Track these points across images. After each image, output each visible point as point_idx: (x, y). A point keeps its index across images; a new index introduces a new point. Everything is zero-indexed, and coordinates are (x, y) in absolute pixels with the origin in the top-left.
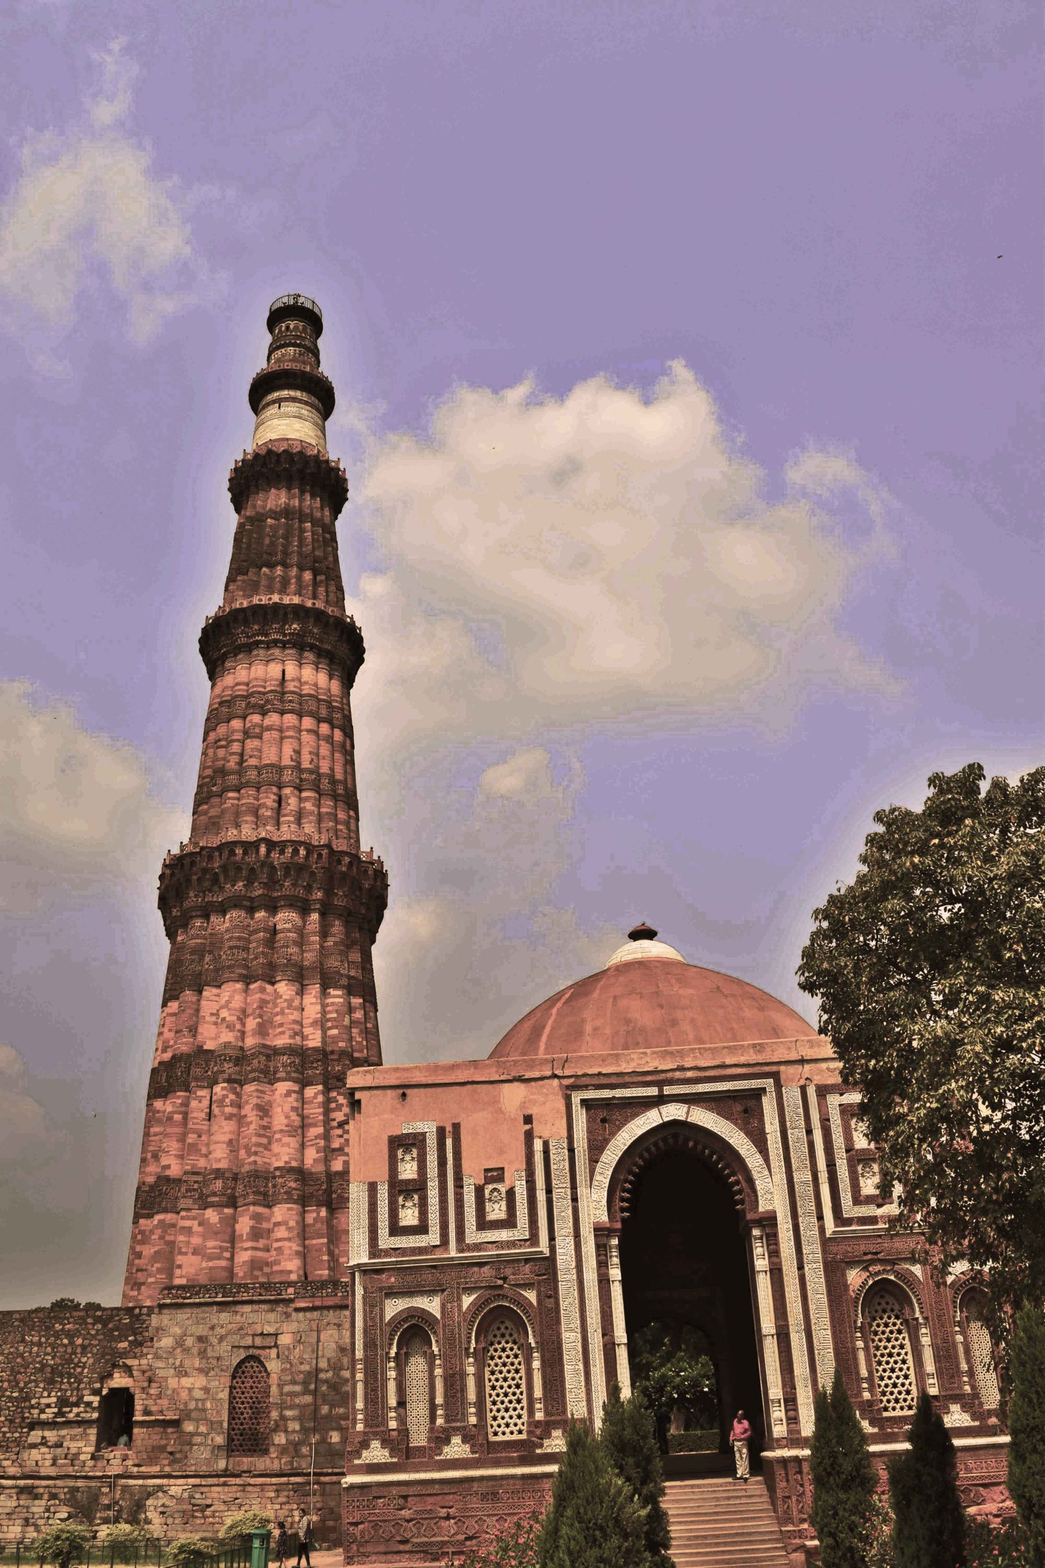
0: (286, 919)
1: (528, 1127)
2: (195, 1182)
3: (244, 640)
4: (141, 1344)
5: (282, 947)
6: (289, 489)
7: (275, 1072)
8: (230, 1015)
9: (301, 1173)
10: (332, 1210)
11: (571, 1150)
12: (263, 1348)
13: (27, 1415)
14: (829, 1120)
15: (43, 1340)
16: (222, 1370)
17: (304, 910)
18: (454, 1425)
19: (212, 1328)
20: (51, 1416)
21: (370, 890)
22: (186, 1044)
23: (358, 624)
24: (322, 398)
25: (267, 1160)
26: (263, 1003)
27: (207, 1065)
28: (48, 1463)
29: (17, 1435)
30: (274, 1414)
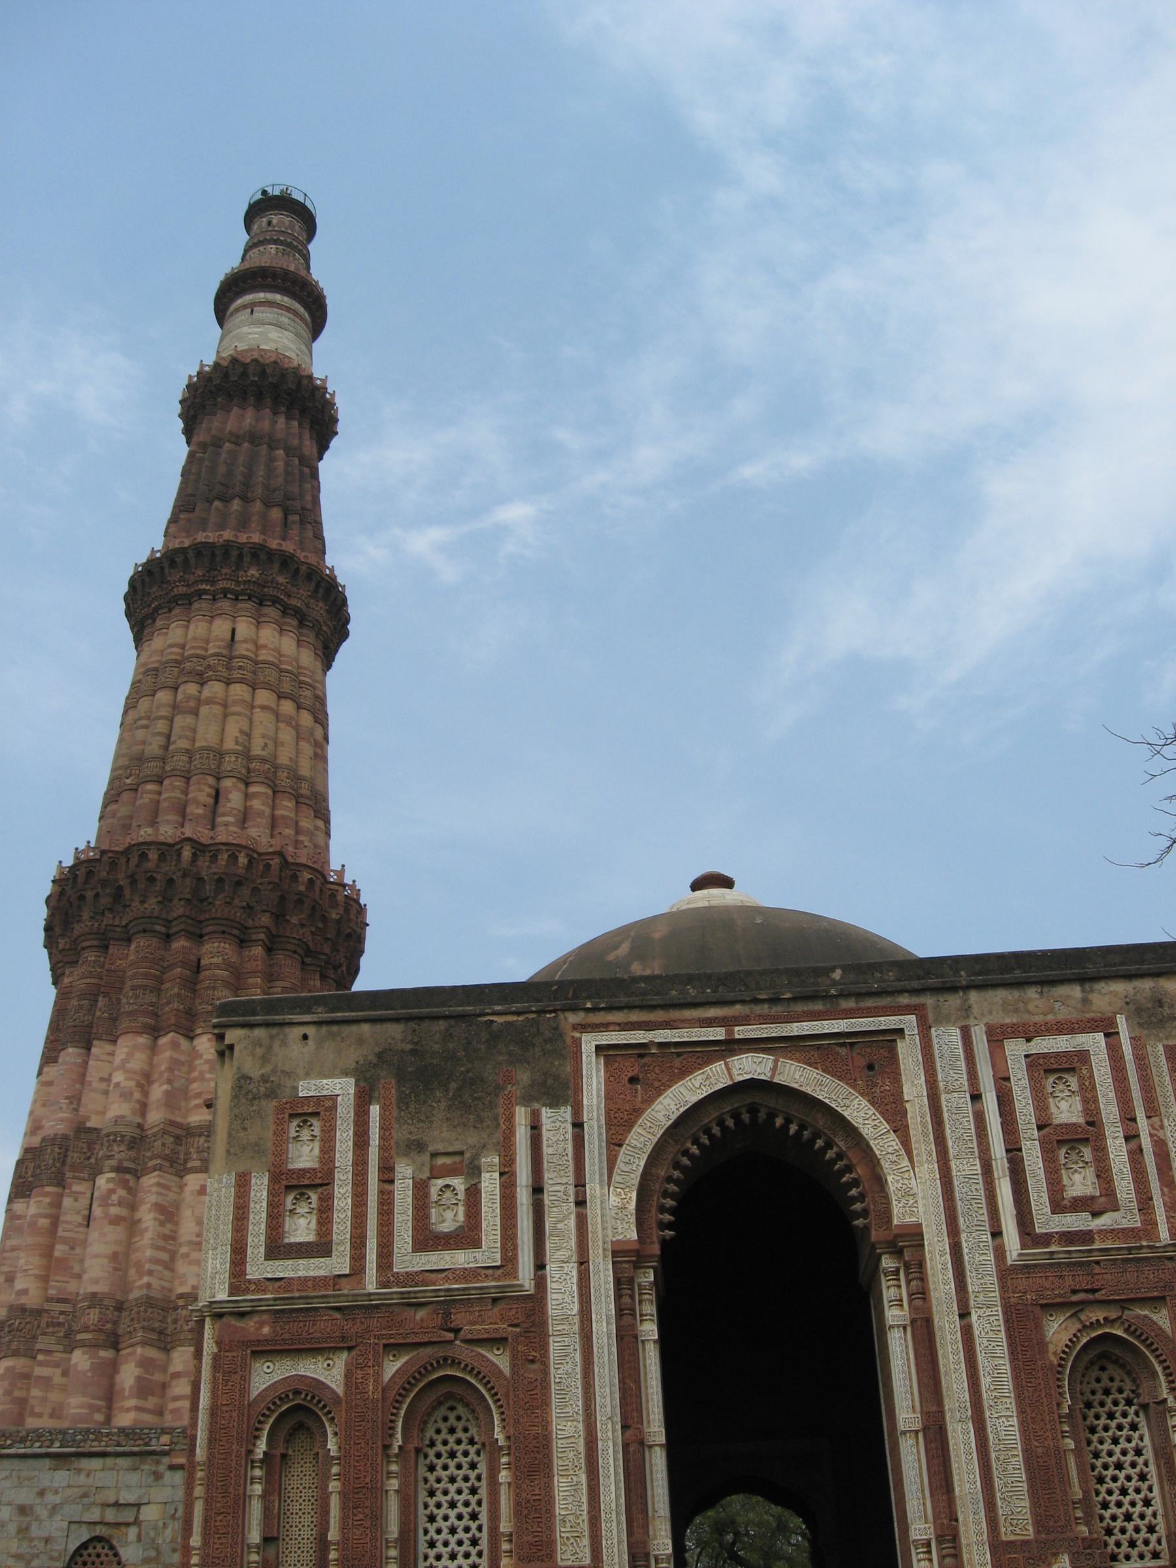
0: (216, 953)
2: (61, 1313)
3: (182, 590)
5: (208, 988)
6: (258, 407)
7: (186, 1161)
8: (126, 1079)
12: (118, 1525)
14: (1008, 1079)
16: (52, 1558)
17: (242, 941)
19: (41, 1493)
21: (339, 921)
22: (62, 1120)
23: (340, 580)
24: (313, 309)
25: (167, 1285)
26: (174, 1064)
27: (89, 1149)
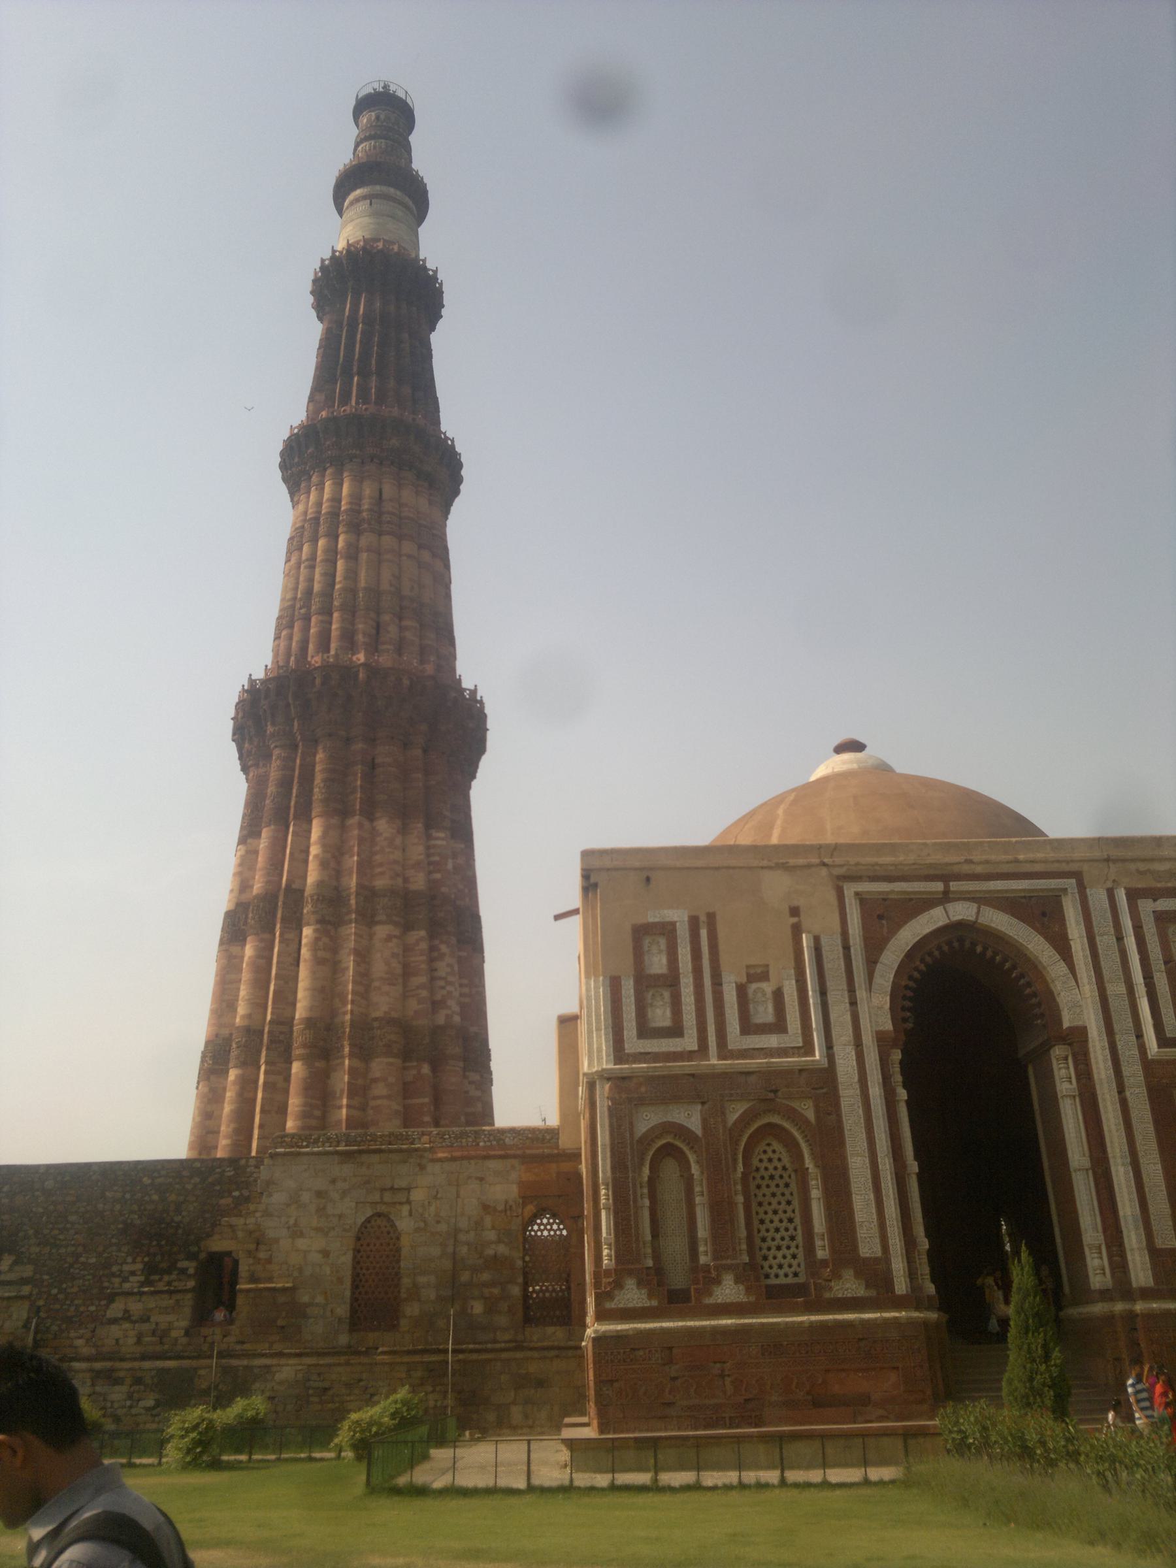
1: (795, 920)
2: (281, 1033)
4: (247, 1200)
9: (404, 1028)
10: (434, 1070)
11: (846, 948)
13: (106, 1284)
15: (128, 1196)
16: (345, 1230)
18: (724, 1262)
19: (333, 1181)
20: (136, 1285)
24: (412, 198)
28: (131, 1341)
29: (92, 1308)
30: (406, 1281)
